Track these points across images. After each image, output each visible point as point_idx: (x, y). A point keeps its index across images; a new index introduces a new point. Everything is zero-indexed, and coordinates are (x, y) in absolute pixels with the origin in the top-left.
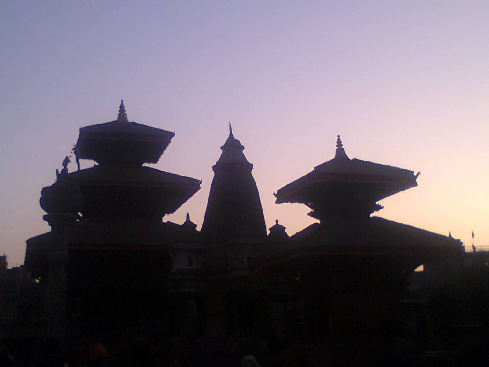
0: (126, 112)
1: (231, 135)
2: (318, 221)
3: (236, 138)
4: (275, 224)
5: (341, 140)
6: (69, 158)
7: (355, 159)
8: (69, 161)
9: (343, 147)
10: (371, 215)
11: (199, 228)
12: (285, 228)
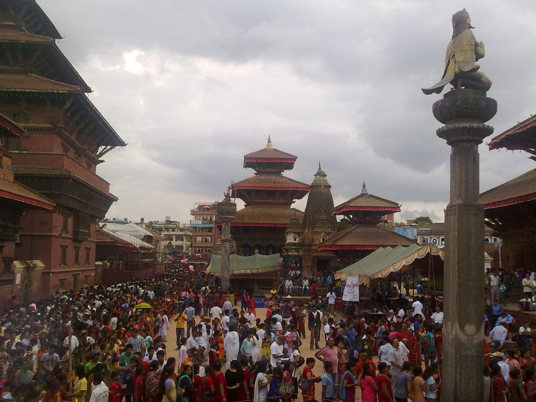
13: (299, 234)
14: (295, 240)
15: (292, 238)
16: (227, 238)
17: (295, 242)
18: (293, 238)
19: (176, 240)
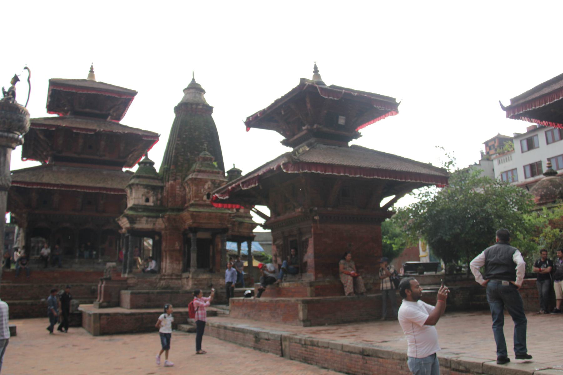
1: (193, 80)
2: (290, 150)
3: (197, 81)
5: (317, 66)
6: (19, 77)
7: (333, 86)
9: (319, 73)
11: (157, 167)
12: (241, 171)
13: (154, 188)
14: (147, 200)
15: (140, 196)
17: (148, 204)
18: (144, 198)
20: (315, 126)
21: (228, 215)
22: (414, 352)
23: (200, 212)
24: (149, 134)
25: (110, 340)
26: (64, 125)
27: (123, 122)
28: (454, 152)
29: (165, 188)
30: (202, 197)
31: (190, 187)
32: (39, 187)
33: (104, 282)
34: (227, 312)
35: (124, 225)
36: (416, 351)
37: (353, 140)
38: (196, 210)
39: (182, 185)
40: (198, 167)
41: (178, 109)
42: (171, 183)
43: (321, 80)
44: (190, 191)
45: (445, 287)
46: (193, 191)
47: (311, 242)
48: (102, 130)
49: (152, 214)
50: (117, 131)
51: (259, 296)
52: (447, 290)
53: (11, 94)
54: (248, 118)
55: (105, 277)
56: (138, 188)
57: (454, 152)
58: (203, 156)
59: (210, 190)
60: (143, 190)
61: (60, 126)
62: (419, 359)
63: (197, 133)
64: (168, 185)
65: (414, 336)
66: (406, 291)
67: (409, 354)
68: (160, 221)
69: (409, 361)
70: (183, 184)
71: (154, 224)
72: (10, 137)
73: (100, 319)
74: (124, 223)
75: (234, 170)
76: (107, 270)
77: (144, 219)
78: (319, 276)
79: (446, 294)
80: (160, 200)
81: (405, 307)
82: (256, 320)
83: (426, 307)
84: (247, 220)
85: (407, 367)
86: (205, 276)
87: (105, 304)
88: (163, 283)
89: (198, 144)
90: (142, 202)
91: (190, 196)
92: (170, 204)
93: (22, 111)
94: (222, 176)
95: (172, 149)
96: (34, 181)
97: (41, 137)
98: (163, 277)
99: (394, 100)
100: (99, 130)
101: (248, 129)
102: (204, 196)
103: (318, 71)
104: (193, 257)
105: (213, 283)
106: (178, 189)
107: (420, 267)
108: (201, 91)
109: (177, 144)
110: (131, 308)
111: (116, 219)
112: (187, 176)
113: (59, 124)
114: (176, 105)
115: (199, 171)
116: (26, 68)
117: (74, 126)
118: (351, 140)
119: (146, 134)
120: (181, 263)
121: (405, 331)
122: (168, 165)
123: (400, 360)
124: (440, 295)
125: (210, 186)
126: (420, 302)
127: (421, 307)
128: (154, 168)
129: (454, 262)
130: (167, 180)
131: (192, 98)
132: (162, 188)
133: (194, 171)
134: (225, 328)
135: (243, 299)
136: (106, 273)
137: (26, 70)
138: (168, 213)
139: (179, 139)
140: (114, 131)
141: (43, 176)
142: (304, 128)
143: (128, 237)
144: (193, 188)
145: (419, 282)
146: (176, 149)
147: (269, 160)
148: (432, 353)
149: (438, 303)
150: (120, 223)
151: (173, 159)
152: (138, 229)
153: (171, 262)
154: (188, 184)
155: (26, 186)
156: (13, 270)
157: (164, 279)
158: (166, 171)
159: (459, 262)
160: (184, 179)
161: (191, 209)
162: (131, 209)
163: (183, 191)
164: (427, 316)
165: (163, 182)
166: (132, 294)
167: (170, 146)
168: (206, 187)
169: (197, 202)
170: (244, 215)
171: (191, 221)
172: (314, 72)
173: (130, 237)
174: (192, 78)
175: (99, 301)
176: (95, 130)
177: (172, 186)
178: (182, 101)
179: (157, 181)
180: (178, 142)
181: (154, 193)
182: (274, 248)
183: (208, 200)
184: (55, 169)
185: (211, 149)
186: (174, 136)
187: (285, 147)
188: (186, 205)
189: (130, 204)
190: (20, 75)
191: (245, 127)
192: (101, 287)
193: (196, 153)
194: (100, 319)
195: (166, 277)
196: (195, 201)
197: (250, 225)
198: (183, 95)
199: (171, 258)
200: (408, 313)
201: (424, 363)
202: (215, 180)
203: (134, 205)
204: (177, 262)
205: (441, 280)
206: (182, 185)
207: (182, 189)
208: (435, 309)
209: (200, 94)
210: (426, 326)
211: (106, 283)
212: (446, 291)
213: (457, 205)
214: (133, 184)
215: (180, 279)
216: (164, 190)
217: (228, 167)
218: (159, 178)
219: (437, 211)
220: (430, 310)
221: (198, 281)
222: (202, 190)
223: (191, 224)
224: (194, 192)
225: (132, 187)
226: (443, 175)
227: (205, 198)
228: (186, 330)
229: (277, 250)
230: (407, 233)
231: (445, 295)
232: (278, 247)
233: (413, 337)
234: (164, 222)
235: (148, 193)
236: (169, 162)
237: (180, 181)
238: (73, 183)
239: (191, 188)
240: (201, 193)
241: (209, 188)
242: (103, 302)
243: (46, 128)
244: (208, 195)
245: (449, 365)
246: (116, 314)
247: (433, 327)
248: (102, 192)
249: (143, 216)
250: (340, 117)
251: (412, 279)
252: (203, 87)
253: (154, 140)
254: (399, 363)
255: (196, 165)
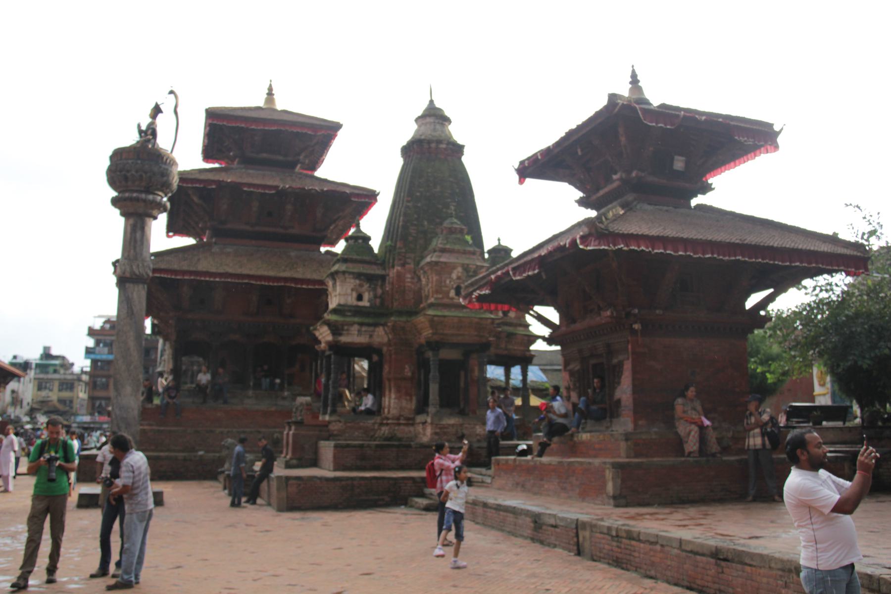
0: (275, 97)
1: (431, 102)
2: (592, 213)
3: (438, 105)
4: (497, 244)
5: (637, 72)
6: (161, 107)
7: (663, 106)
8: (160, 111)
9: (640, 84)
10: (694, 202)
11: (375, 244)
12: (511, 250)
13: (370, 279)
14: (360, 298)
15: (349, 291)
16: (137, 272)
17: (361, 304)
18: (355, 295)
19: (60, 390)
20: (634, 174)
21: (489, 321)
22: (812, 559)
23: (444, 316)
24: (361, 192)
25: (303, 519)
26: (229, 180)
27: (320, 173)
28: (879, 213)
29: (387, 278)
30: (448, 293)
31: (428, 276)
32: (192, 278)
33: (293, 428)
34: (489, 480)
35: (324, 337)
36: (817, 557)
37: (699, 196)
38: (439, 313)
39: (415, 272)
40: (441, 243)
41: (407, 151)
42: (397, 270)
43: (643, 97)
44: (429, 283)
45: (871, 448)
46: (432, 282)
47: (628, 366)
48: (287, 186)
49: (367, 320)
50: (310, 188)
51: (540, 455)
52: (875, 453)
53: (149, 134)
54: (522, 163)
55: (293, 419)
56: (345, 279)
57: (879, 213)
58: (449, 226)
59: (461, 281)
60: (352, 281)
61: (223, 181)
62: (821, 571)
63: (438, 189)
64: (393, 273)
65: (813, 529)
66: (798, 451)
67: (802, 562)
68: (380, 330)
69: (802, 575)
70: (417, 272)
71: (371, 336)
72: (149, 200)
73: (287, 485)
74: (324, 335)
75: (500, 247)
76: (297, 409)
77: (356, 327)
78: (640, 423)
79: (874, 461)
80: (380, 297)
81: (795, 479)
82: (535, 494)
83: (834, 482)
84: (520, 331)
85: (801, 585)
86: (452, 421)
87: (294, 462)
88: (385, 430)
89: (440, 206)
90: (352, 300)
91: (429, 291)
92: (395, 304)
93: (167, 159)
94: (480, 258)
95: (398, 214)
96: (185, 268)
97: (195, 199)
98: (385, 422)
99: (771, 125)
100: (283, 187)
101: (521, 181)
102: (450, 290)
103: (638, 81)
104: (434, 389)
105: (465, 432)
106: (409, 280)
107: (815, 413)
108: (445, 120)
109: (407, 207)
110: (335, 470)
111: (311, 328)
112: (422, 258)
113: (221, 179)
114: (405, 143)
115: (443, 251)
116: (171, 92)
117: (245, 180)
118: (696, 196)
119: (356, 192)
120: (414, 398)
121: (795, 521)
122: (392, 240)
123: (783, 570)
124: (862, 463)
125: (460, 274)
126: (822, 472)
127: (824, 481)
128: (370, 245)
129: (878, 406)
130: (391, 264)
131: (429, 132)
132: (383, 278)
133: (435, 251)
134: (485, 505)
135: (515, 460)
136: (295, 413)
137: (172, 95)
138: (393, 318)
139: (410, 199)
140: (306, 188)
141: (199, 260)
142: (615, 177)
143: (329, 356)
144: (432, 278)
145: (822, 438)
146: (405, 215)
147: (557, 232)
148: (846, 562)
149: (857, 476)
150: (317, 334)
151: (400, 230)
152: (345, 343)
153: (398, 398)
154: (425, 272)
155: (173, 277)
156: (157, 405)
157: (387, 424)
158: (390, 251)
159: (888, 405)
160: (418, 263)
161: (430, 312)
162: (335, 311)
163: (417, 282)
164: (837, 497)
165: (384, 269)
166: (336, 446)
167: (395, 210)
168: (454, 276)
169: (439, 301)
170: (515, 321)
171: (430, 331)
172: (631, 83)
173: (333, 356)
174: (430, 99)
175: (285, 457)
176: (276, 187)
177: (399, 275)
178: (413, 138)
179: (375, 267)
180: (408, 204)
181: (370, 287)
182: (566, 375)
183: (457, 297)
184: (215, 249)
185: (462, 214)
186: (402, 194)
187: (583, 209)
188: (422, 306)
189: (333, 304)
190: (163, 103)
191: (517, 177)
192: (288, 434)
193: (438, 220)
194: (287, 485)
195: (389, 422)
196: (436, 299)
197: (526, 338)
198: (415, 127)
199: (398, 391)
200: (800, 490)
201: (831, 580)
202: (468, 265)
203: (339, 305)
204: (408, 398)
205: (864, 436)
206: (415, 272)
207: (416, 280)
208: (851, 486)
209: (443, 125)
210: (835, 514)
211: (296, 430)
212: (873, 454)
213: (885, 307)
214: (337, 272)
215: (413, 425)
216: (387, 282)
217: (489, 244)
218: (378, 262)
219: (847, 316)
220: (842, 487)
221: (440, 428)
222: (448, 282)
223: (430, 335)
224: (434, 284)
225: (335, 276)
226: (859, 254)
227: (452, 293)
228: (422, 506)
229: (571, 380)
230: (793, 353)
231: (870, 463)
232: (572, 374)
233: (812, 533)
234: (386, 333)
235: (361, 286)
236: (395, 236)
237: (412, 266)
238: (245, 271)
239: (430, 277)
240: (446, 286)
241: (459, 278)
242: (291, 459)
243: (202, 186)
244: (458, 291)
245: (875, 586)
246: (311, 478)
247: (847, 518)
248: (288, 284)
249: (354, 323)
250: (676, 157)
251: (810, 432)
252: (447, 113)
253: (370, 201)
254: (781, 576)
255: (437, 243)
